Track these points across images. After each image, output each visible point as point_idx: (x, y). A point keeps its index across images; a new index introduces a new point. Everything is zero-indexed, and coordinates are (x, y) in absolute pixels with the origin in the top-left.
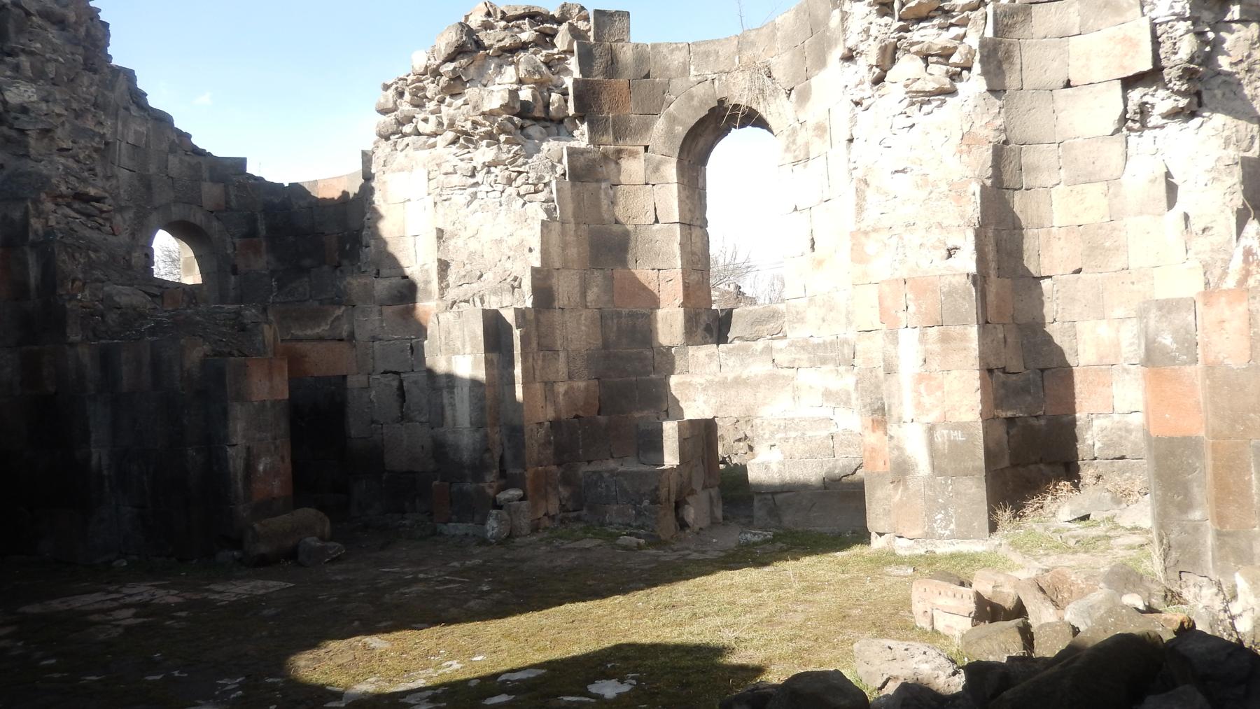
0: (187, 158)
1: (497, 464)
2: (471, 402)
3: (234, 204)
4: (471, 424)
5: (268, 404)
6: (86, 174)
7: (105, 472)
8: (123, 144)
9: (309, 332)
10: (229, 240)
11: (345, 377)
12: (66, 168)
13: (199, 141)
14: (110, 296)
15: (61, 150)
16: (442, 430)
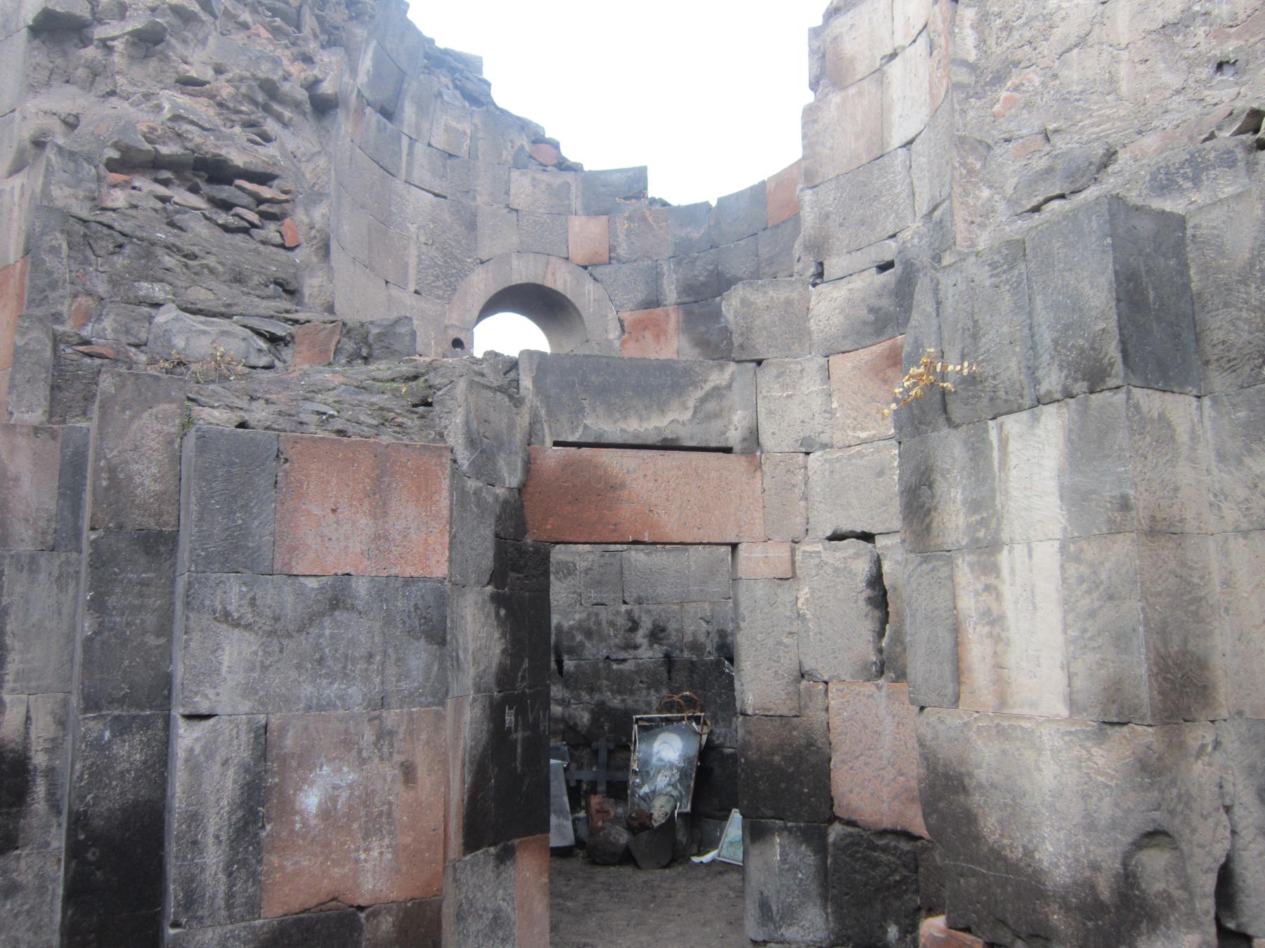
0: (545, 177)
1: (1207, 904)
2: (1067, 605)
3: (622, 251)
4: (1072, 703)
5: (361, 588)
6: (237, 129)
7: (39, 759)
8: (420, 148)
9: (634, 427)
10: (612, 315)
11: (734, 546)
12: (175, 105)
13: (570, 152)
14: (166, 335)
15: (187, 83)
16: (953, 719)
